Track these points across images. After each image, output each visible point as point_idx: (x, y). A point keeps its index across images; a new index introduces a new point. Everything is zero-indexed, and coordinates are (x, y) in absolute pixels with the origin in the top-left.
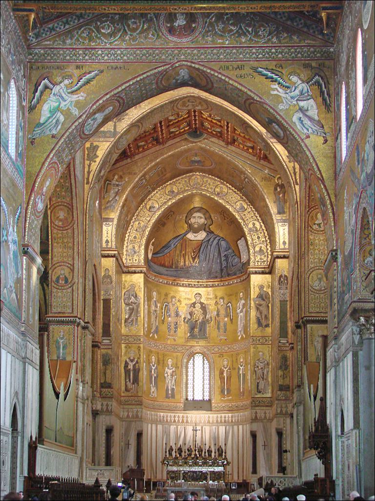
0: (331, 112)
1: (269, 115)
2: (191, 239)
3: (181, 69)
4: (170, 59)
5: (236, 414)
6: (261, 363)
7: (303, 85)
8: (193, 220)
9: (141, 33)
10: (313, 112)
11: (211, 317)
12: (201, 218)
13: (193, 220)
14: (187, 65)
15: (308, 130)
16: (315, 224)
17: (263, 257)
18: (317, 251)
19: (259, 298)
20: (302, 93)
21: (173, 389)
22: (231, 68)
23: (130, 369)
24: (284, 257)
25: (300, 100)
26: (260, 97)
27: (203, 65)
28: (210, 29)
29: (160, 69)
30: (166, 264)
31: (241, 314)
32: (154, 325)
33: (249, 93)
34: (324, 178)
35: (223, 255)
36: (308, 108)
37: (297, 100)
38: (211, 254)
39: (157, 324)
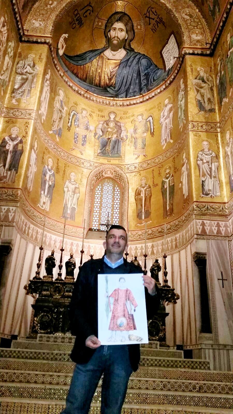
2: (110, 58)
5: (160, 242)
6: (206, 155)
8: (112, 33)
11: (127, 136)
12: (122, 30)
13: (112, 33)
19: (199, 79)
21: (73, 209)
23: (8, 150)
30: (79, 75)
31: (166, 121)
32: (56, 123)
35: (142, 74)
38: (129, 76)
39: (61, 126)
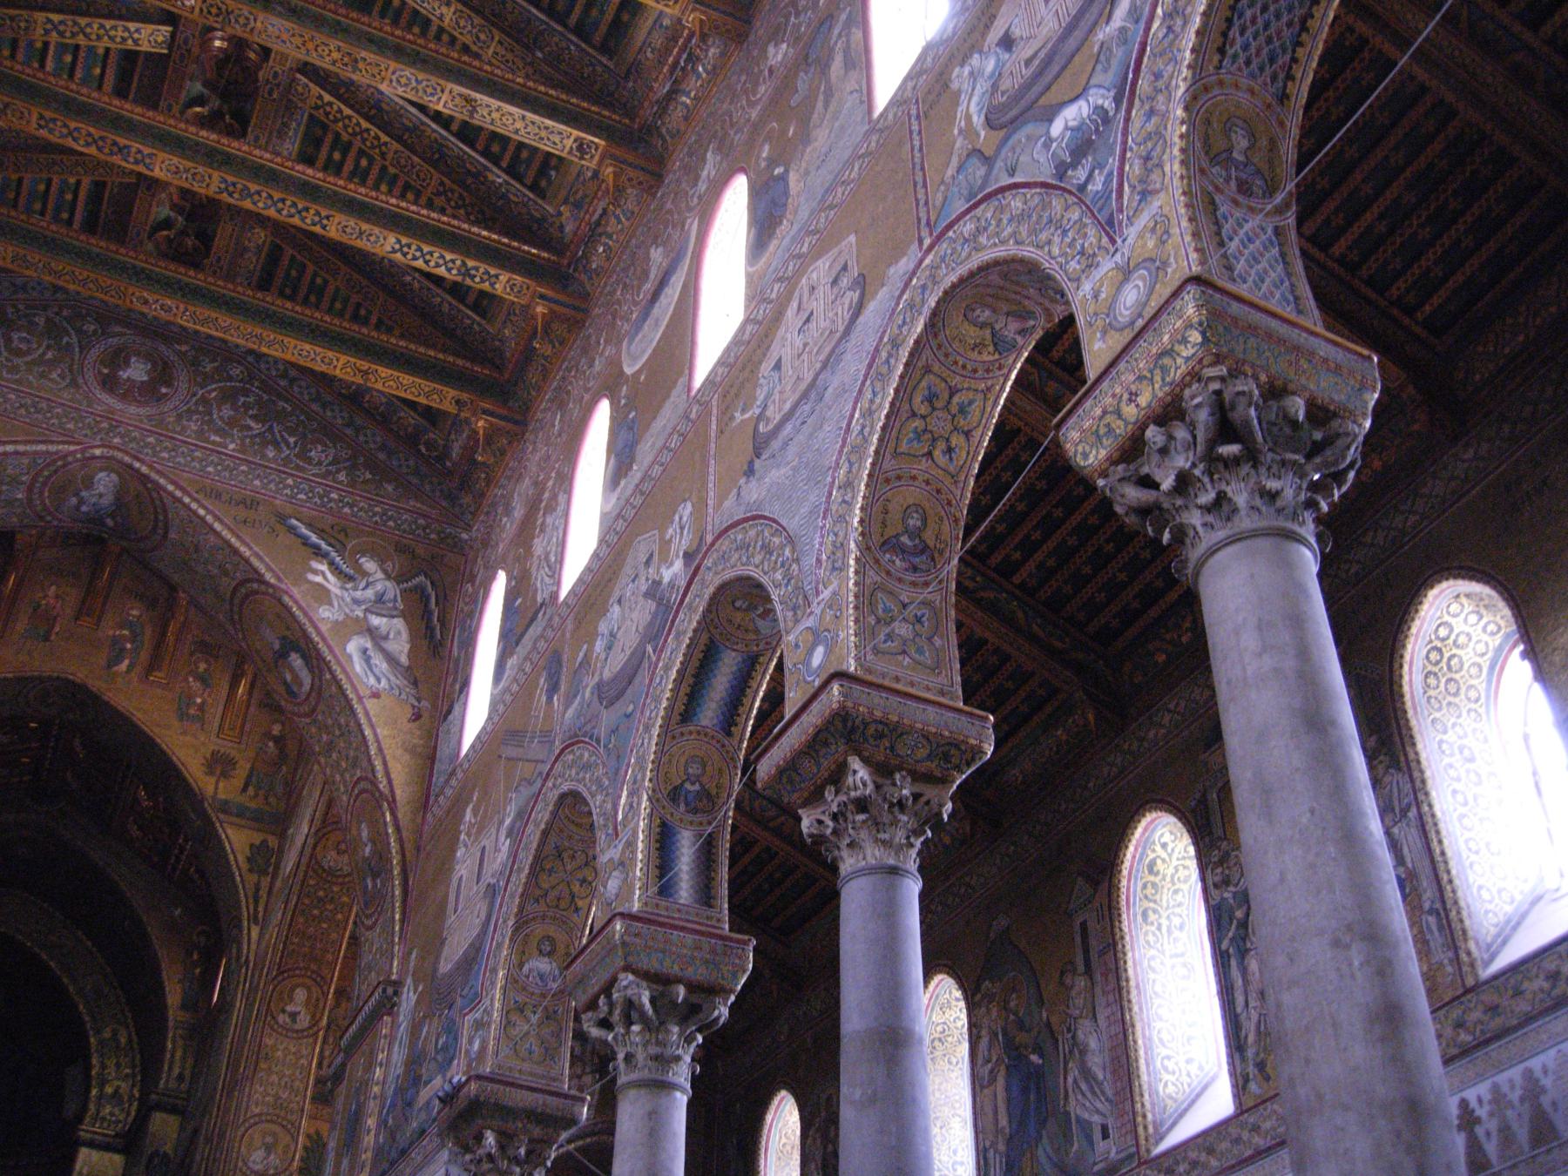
0: (441, 658)
1: (288, 628)
3: (101, 470)
4: (86, 436)
7: (388, 584)
9: (33, 362)
10: (400, 646)
14: (120, 462)
15: (379, 680)
16: (284, 1011)
17: (117, 1111)
18: (274, 1078)
20: (380, 599)
22: (225, 497)
24: (173, 1110)
25: (372, 613)
26: (279, 579)
27: (158, 472)
28: (201, 409)
29: (52, 448)
33: (256, 562)
34: (398, 798)
36: (388, 633)
37: (366, 610)
